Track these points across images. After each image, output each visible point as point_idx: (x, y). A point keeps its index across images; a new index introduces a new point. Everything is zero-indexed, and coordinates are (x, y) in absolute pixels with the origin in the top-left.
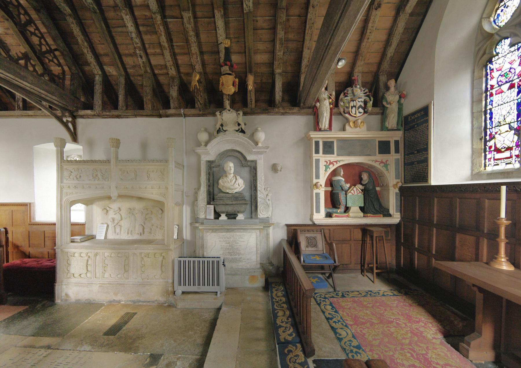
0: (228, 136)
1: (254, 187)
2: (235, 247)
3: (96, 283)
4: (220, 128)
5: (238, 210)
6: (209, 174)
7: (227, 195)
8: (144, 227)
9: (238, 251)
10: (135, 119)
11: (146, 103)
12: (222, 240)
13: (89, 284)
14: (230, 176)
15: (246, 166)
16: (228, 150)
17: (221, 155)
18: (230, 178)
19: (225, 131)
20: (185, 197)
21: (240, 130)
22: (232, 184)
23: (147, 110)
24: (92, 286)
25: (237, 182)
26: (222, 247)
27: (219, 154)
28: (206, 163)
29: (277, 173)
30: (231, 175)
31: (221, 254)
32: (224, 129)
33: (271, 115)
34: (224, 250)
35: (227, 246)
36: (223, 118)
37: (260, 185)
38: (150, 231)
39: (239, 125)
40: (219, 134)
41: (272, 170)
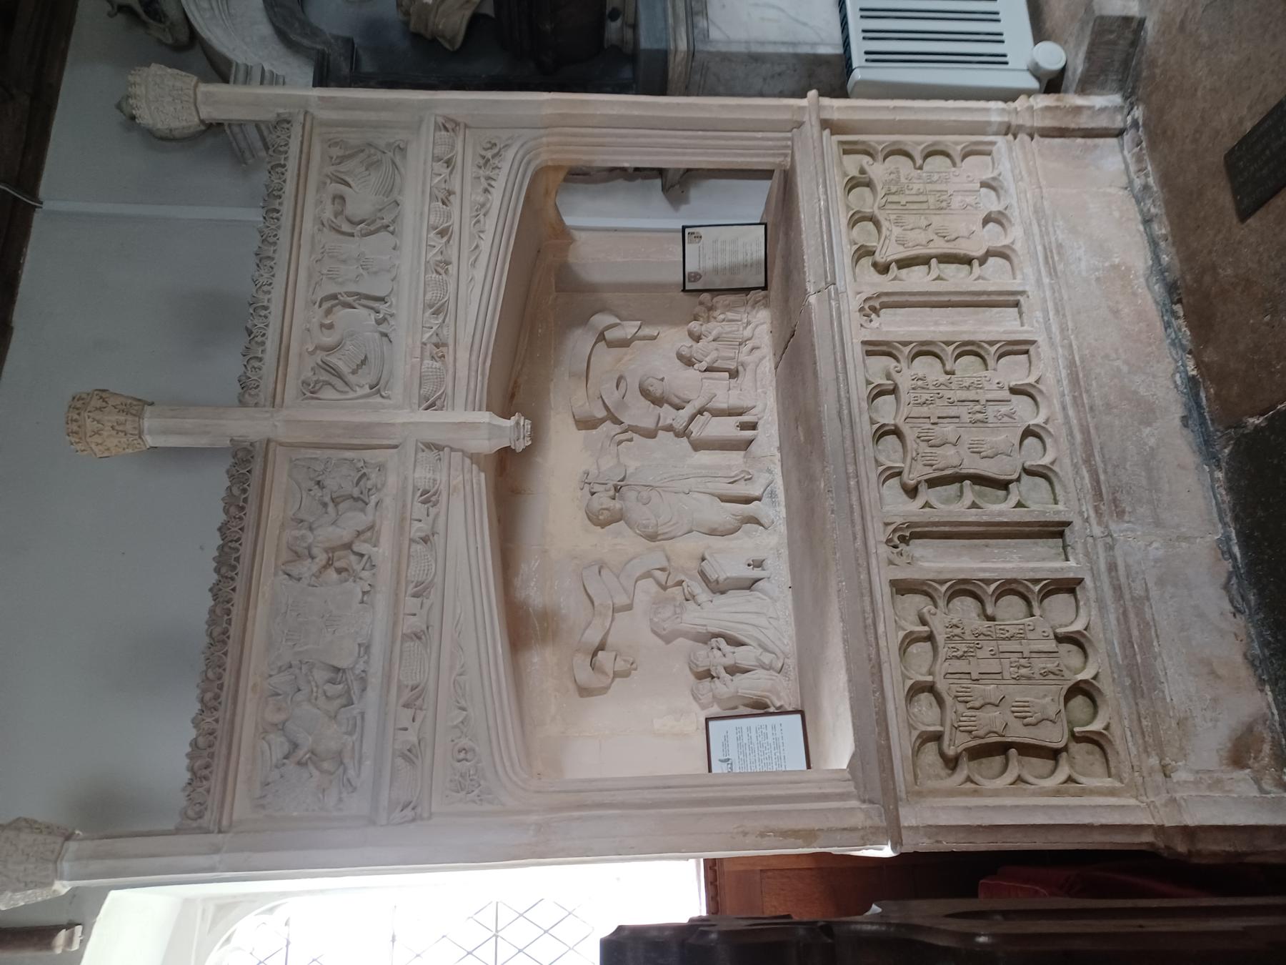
8: (700, 412)
13: (1117, 589)
24: (1127, 566)
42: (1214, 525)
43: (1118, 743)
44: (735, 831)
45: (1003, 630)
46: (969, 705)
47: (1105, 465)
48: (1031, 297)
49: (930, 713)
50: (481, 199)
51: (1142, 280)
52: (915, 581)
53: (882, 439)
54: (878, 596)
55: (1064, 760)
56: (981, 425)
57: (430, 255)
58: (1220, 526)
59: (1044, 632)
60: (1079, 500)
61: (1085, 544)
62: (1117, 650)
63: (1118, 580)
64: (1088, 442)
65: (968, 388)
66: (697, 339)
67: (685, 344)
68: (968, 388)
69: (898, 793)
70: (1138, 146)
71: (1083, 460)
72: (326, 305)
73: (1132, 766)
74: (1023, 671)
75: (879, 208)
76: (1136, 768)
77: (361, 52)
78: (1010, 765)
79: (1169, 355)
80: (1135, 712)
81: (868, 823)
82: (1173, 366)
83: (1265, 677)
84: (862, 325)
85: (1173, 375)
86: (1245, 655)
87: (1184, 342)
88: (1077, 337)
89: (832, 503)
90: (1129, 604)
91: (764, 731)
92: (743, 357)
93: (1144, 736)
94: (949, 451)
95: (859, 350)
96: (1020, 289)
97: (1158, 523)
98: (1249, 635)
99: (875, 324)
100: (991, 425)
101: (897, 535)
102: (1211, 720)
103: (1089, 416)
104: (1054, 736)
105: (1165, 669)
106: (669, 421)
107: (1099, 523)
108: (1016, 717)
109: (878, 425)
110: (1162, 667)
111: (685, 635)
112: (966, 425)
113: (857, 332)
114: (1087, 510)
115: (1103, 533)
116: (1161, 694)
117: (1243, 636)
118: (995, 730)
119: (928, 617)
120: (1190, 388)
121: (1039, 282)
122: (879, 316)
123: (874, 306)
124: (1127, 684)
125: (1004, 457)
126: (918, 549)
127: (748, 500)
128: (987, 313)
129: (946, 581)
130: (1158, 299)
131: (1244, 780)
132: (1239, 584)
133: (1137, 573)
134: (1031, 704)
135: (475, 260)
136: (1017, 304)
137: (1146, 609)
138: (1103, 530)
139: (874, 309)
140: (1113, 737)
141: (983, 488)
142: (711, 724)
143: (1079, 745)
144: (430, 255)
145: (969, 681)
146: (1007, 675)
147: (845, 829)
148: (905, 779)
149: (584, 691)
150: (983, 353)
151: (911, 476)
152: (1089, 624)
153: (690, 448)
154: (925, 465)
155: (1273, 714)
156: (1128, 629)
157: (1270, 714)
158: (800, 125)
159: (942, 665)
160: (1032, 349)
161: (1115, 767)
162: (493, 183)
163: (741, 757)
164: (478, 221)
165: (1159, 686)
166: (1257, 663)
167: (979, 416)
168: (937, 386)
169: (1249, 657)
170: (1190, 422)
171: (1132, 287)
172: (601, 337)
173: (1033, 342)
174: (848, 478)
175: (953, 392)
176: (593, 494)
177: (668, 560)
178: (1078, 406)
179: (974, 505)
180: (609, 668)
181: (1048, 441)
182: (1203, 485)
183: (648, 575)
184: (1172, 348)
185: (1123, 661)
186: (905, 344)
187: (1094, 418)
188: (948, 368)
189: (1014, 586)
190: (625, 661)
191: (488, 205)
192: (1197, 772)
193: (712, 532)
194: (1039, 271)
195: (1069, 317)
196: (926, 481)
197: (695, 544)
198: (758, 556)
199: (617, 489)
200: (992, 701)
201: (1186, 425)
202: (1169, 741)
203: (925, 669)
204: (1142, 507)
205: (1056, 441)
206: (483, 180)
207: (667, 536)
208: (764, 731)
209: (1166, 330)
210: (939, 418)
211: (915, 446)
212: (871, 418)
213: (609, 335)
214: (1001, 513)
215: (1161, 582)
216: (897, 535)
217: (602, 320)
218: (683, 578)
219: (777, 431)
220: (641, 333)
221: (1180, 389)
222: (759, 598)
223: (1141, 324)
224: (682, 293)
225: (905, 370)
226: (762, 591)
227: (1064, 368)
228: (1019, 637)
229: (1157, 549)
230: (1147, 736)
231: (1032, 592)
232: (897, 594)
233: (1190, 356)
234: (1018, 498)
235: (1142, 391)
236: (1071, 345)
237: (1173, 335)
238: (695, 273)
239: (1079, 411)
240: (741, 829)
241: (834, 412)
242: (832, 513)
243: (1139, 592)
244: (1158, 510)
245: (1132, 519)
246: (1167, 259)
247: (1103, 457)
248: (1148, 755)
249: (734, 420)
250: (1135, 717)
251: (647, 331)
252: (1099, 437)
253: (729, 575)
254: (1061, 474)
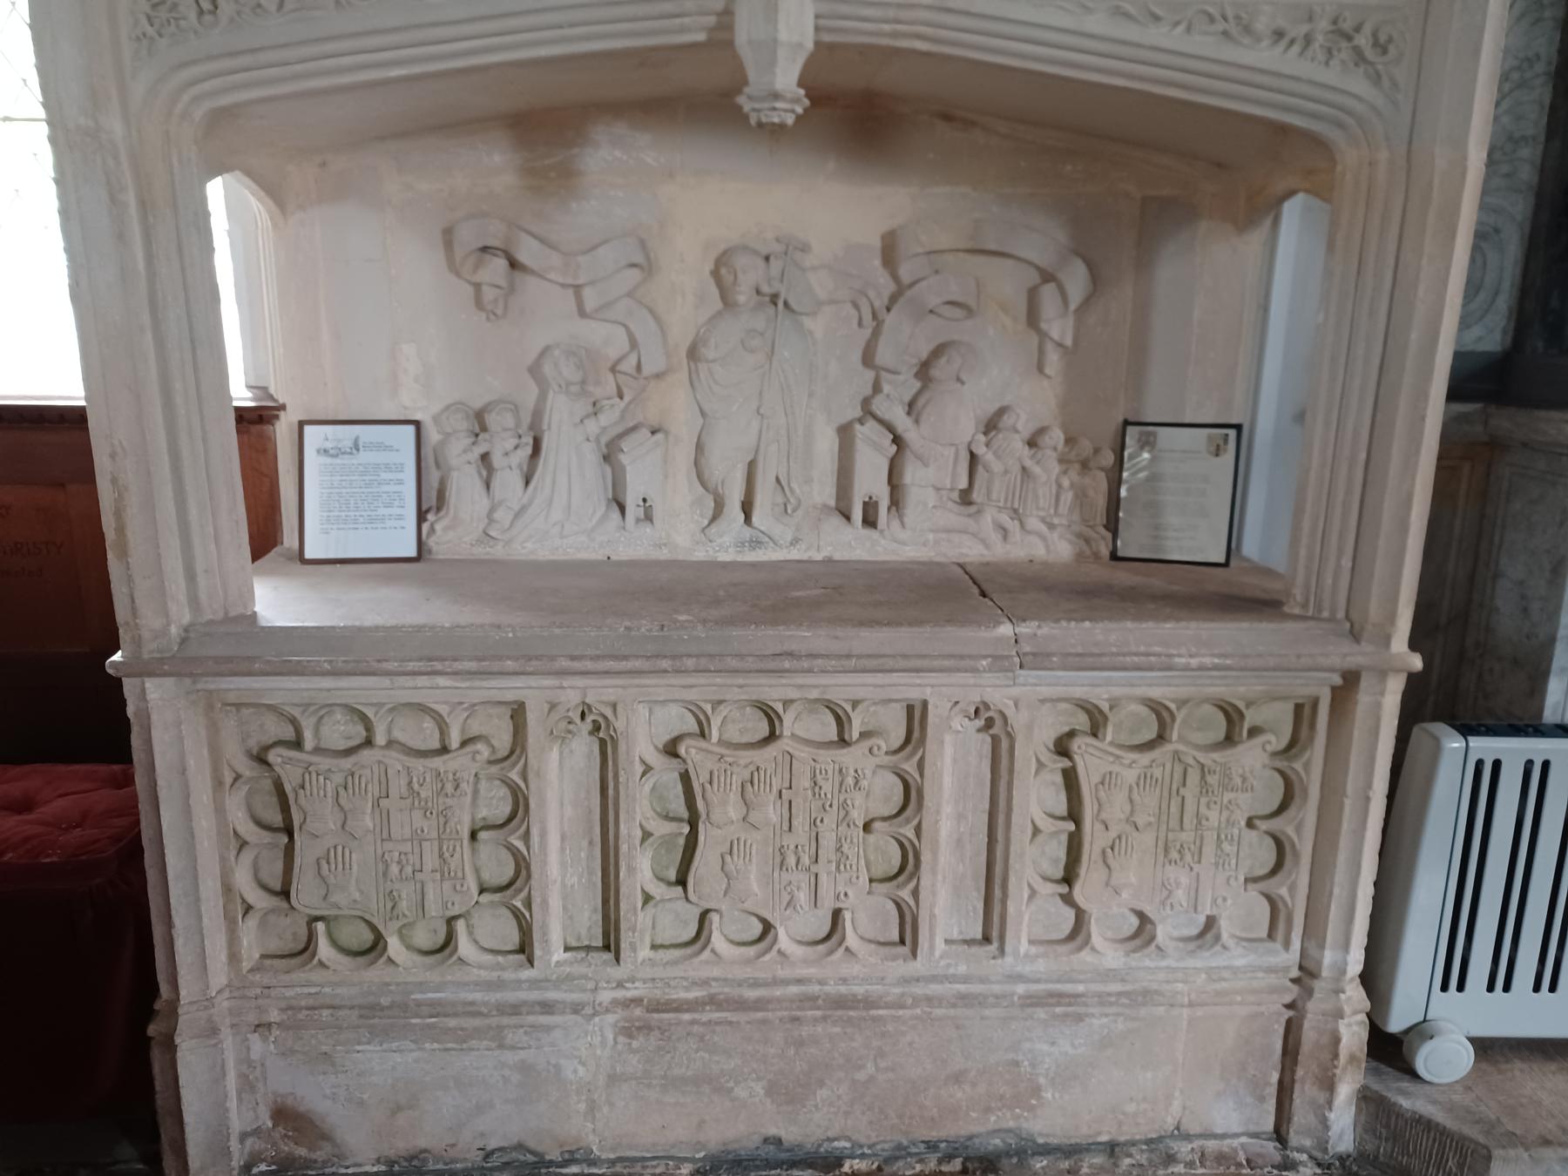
3: (576, 997)
8: (897, 440)
13: (515, 1009)
24: (548, 1029)
42: (613, 1150)
43: (299, 976)
44: (116, 443)
45: (454, 850)
46: (342, 791)
47: (704, 1024)
48: (992, 962)
49: (336, 735)
50: (1262, 25)
51: (1011, 1124)
52: (525, 740)
53: (762, 714)
54: (494, 683)
55: (275, 904)
56: (778, 860)
58: (612, 1156)
59: (453, 904)
60: (653, 979)
61: (586, 977)
62: (430, 995)
63: (528, 1014)
64: (742, 1005)
65: (839, 849)
66: (1032, 443)
67: (1023, 421)
68: (839, 849)
69: (205, 679)
70: (1248, 1161)
71: (715, 994)
73: (269, 988)
74: (394, 869)
75: (1176, 752)
76: (265, 991)
78: (264, 833)
79: (882, 1138)
80: (343, 1003)
81: (146, 634)
82: (863, 1140)
83: (396, 1168)
84: (957, 703)
85: (848, 1139)
86: (426, 1151)
87: (900, 1163)
88: (917, 1018)
89: (643, 630)
90: (494, 1021)
91: (396, 503)
92: (988, 517)
93: (308, 1008)
94: (734, 811)
95: (914, 695)
96: (1008, 948)
97: (613, 1079)
98: (454, 1161)
99: (958, 722)
100: (776, 874)
101: (601, 720)
102: (334, 1094)
103: (785, 1013)
104: (306, 895)
105: (401, 1051)
106: (886, 388)
107: (616, 1002)
108: (329, 850)
109: (709, 712)
110: (403, 1047)
111: (542, 397)
112: (777, 838)
113: (939, 692)
114: (636, 988)
115: (600, 1004)
116: (364, 1040)
117: (452, 1153)
118: (308, 820)
119: (469, 749)
120: (826, 1157)
121: (1020, 978)
122: (979, 730)
123: (989, 720)
124: (382, 1001)
125: (724, 886)
126: (583, 747)
127: (747, 508)
128: (975, 894)
129: (525, 780)
130: (977, 1141)
131: (257, 1118)
132: (525, 1164)
133: (539, 1040)
134: (347, 871)
135: (1127, 15)
136: (987, 939)
137: (485, 1042)
138: (605, 1004)
139: (989, 723)
140: (311, 970)
141: (681, 850)
142: (411, 429)
143: (305, 924)
145: (377, 794)
146: (388, 846)
147: (133, 601)
148: (230, 690)
149: (448, 235)
150: (901, 879)
151: (693, 751)
152: (469, 965)
153: (843, 420)
154: (711, 773)
155: (347, 1167)
156: (456, 1015)
157: (347, 1164)
158: (1355, 635)
159: (398, 760)
160: (905, 950)
161: (272, 966)
162: (1296, 49)
163: (361, 468)
164: (1212, 20)
165: (377, 1040)
166: (415, 1163)
167: (791, 860)
168: (844, 805)
169: (423, 1155)
170: (772, 1147)
171: (1000, 1110)
172: (1047, 277)
173: (914, 954)
174: (674, 657)
175: (834, 826)
176: (767, 259)
177: (658, 376)
178: (801, 1001)
179: (646, 835)
180: (484, 276)
181: (751, 951)
182: (673, 1146)
183: (634, 344)
184: (892, 1145)
185: (414, 1000)
186: (921, 766)
187: (781, 1020)
188: (877, 825)
189: (524, 872)
190: (496, 300)
191: (1246, 40)
192: (263, 1065)
193: (699, 447)
194: (1038, 981)
195: (952, 1012)
196: (687, 771)
197: (684, 424)
198: (657, 514)
199: (774, 299)
200: (349, 822)
201: (766, 1140)
202: (301, 1039)
203: (398, 734)
204: (639, 1062)
205: (748, 962)
206: (1304, 28)
207: (694, 376)
208: (396, 503)
209: (923, 1142)
210: (790, 802)
211: (742, 762)
212: (792, 701)
213: (1048, 293)
214: (631, 870)
215: (525, 1068)
216: (601, 720)
217: (1076, 280)
218: (627, 398)
219: (858, 558)
220: (1049, 347)
221: (825, 1145)
222: (594, 512)
223: (935, 1110)
224: (1121, 419)
225: (873, 761)
226: (604, 518)
227: (867, 991)
228: (443, 871)
229: (575, 1071)
230: (308, 1012)
231: (514, 896)
232: (513, 709)
233: (875, 1166)
234: (658, 898)
235: (823, 1093)
236: (902, 1007)
237: (914, 1150)
238: (1155, 441)
239: (792, 1001)
240: (119, 450)
241: (794, 647)
242: (628, 629)
243: (510, 1038)
244: (634, 1082)
245: (620, 1047)
246: (1038, 1165)
247: (717, 1023)
248: (283, 1010)
249: (882, 494)
250: (337, 1002)
251: (1053, 358)
252: (749, 1023)
253: (628, 469)
254: (696, 960)
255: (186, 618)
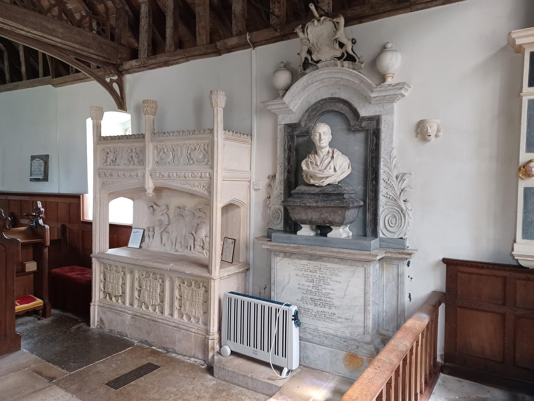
0: (321, 72)
1: (372, 174)
2: (324, 291)
4: (306, 59)
5: (330, 219)
6: (290, 149)
7: (313, 188)
9: (328, 300)
10: (188, 63)
11: (200, 34)
12: (300, 273)
14: (322, 152)
15: (355, 131)
16: (322, 100)
17: (312, 111)
18: (322, 156)
19: (318, 62)
20: (252, 190)
21: (346, 55)
22: (322, 169)
23: (200, 45)
24: (125, 315)
25: (332, 165)
26: (300, 286)
27: (307, 111)
28: (285, 129)
29: (429, 141)
30: (323, 150)
31: (298, 300)
32: (315, 58)
33: (418, 10)
34: (304, 293)
35: (309, 286)
36: (310, 37)
37: (386, 169)
38: (202, 245)
39: (341, 45)
40: (307, 71)
41: (416, 136)
57: (179, 173)
72: (172, 149)
77: (308, 137)
92: (204, 251)
97: (131, 325)
144: (179, 173)
215: (122, 320)
255: (99, 251)
